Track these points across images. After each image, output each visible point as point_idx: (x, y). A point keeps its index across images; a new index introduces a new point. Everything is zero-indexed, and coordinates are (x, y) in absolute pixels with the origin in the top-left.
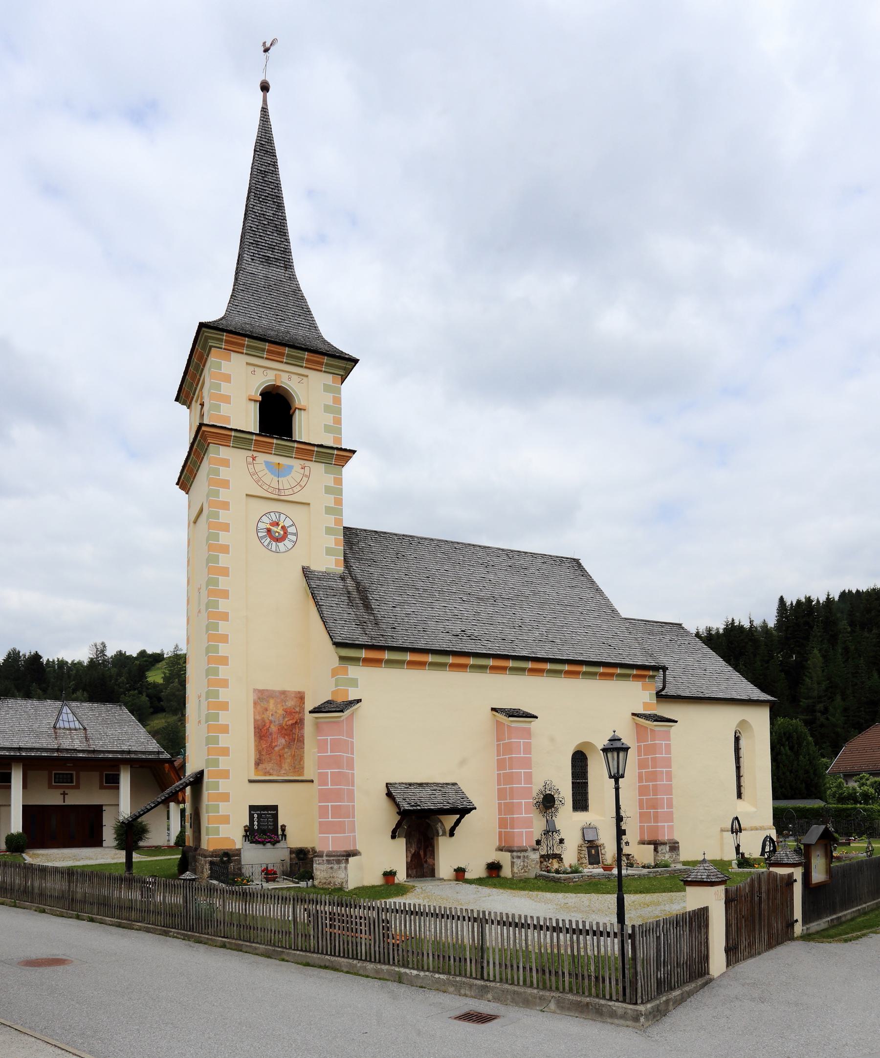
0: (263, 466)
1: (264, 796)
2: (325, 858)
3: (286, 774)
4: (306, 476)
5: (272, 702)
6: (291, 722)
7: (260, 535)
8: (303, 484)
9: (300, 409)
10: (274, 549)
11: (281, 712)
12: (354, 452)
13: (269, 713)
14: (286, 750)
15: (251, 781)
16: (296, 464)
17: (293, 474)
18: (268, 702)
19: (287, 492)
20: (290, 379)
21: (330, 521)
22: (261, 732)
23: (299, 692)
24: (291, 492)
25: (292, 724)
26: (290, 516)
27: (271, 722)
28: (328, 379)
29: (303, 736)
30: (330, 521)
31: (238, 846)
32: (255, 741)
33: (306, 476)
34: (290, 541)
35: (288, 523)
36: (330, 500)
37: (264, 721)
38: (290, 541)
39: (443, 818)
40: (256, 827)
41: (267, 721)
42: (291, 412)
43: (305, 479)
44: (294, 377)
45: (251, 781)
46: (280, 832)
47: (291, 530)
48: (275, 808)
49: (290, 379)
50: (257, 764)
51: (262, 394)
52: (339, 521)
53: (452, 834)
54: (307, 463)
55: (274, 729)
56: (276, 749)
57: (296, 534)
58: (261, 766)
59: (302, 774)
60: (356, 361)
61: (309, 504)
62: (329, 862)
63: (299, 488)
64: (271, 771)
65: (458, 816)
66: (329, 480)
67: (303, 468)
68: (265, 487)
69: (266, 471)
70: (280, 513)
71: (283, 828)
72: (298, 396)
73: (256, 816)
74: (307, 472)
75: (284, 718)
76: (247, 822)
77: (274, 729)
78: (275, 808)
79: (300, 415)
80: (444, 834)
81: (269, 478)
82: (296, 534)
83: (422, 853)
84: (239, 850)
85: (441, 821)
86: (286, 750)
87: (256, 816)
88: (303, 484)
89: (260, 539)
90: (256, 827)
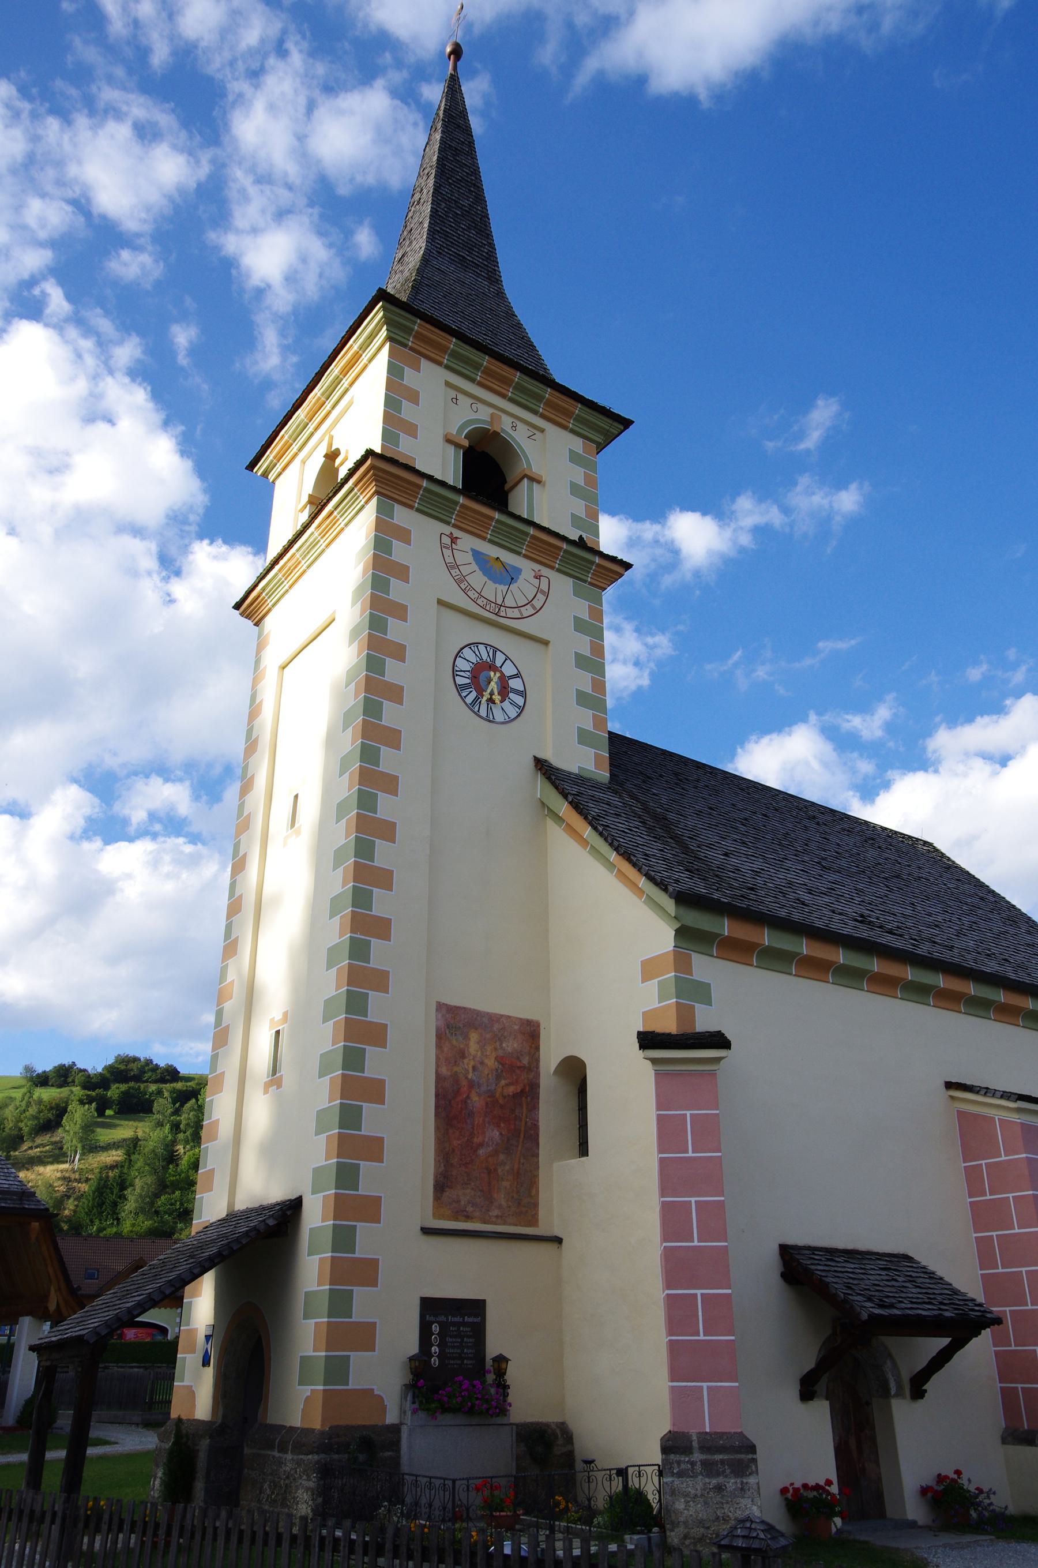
0: (469, 558)
1: (458, 1271)
2: (697, 1456)
3: (502, 1219)
4: (543, 592)
5: (474, 1037)
6: (511, 1090)
7: (460, 681)
8: (537, 604)
9: (532, 479)
10: (483, 712)
11: (491, 1062)
13: (468, 1063)
14: (502, 1157)
15: (426, 1231)
16: (527, 568)
17: (521, 582)
18: (466, 1037)
19: (510, 613)
22: (451, 1106)
23: (529, 1022)
24: (516, 613)
25: (515, 1096)
27: (471, 1084)
28: (577, 444)
29: (535, 1127)
31: (391, 1417)
32: (437, 1128)
33: (543, 592)
34: (513, 704)
35: (508, 670)
36: (583, 644)
37: (455, 1077)
38: (513, 704)
39: (892, 1343)
40: (435, 1361)
41: (464, 1083)
42: (507, 487)
43: (541, 597)
44: (520, 426)
45: (426, 1231)
46: (490, 1378)
48: (477, 1307)
50: (441, 1186)
53: (918, 1393)
54: (545, 571)
55: (476, 1101)
56: (481, 1152)
57: (523, 694)
58: (448, 1194)
59: (533, 1222)
60: (627, 423)
61: (546, 643)
62: (710, 1469)
63: (528, 611)
64: (470, 1209)
65: (946, 1341)
66: (582, 608)
67: (538, 577)
68: (473, 594)
69: (474, 567)
70: (496, 650)
71: (501, 1360)
72: (526, 456)
73: (435, 1328)
74: (544, 587)
75: (498, 1078)
76: (414, 1349)
77: (476, 1101)
78: (477, 1307)
79: (530, 490)
80: (899, 1394)
81: (477, 579)
82: (523, 694)
83: (853, 1444)
84: (396, 1429)
85: (890, 1356)
86: (502, 1157)
87: (435, 1328)
89: (460, 688)
90: (435, 1361)
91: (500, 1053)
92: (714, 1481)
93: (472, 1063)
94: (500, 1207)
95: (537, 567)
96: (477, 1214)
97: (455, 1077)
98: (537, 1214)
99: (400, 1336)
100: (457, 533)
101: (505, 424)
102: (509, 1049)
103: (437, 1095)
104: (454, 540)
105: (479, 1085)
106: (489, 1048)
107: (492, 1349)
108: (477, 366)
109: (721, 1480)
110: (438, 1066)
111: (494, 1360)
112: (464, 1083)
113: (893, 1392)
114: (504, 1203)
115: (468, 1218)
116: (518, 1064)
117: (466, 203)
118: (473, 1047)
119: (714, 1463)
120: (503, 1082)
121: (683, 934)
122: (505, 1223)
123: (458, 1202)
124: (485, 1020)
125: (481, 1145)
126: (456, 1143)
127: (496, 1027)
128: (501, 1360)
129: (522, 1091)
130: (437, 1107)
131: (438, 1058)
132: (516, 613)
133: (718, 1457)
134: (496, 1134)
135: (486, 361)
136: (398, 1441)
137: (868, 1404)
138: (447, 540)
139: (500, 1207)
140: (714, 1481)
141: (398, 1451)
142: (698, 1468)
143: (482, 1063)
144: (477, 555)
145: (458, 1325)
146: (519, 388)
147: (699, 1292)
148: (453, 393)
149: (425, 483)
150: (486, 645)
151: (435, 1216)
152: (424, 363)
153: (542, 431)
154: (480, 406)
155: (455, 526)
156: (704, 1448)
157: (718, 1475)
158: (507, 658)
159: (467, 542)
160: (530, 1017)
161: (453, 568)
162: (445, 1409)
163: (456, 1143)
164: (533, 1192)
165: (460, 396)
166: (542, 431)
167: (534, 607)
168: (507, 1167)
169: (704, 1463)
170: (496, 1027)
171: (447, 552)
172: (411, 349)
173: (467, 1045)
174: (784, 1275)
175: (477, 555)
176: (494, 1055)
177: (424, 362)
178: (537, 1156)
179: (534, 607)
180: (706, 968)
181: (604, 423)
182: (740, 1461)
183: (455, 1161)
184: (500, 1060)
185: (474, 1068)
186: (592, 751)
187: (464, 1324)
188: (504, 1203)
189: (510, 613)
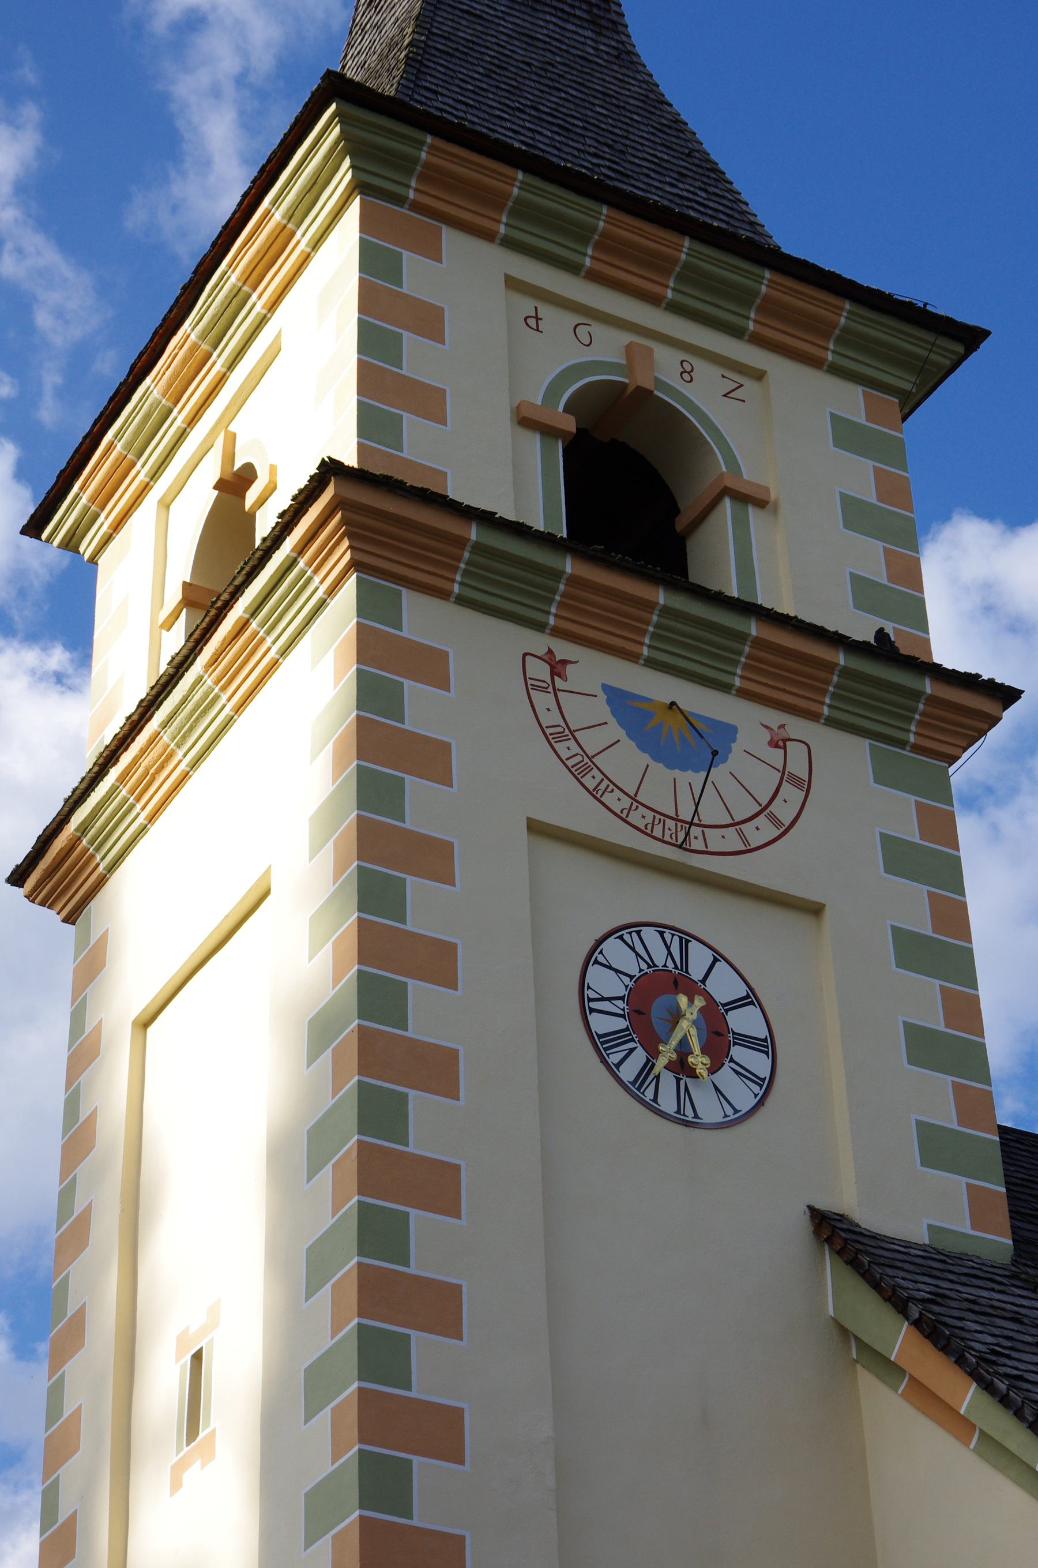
7: (601, 1024)
8: (784, 812)
10: (668, 1102)
16: (749, 721)
17: (736, 760)
19: (716, 840)
20: (687, 374)
26: (738, 951)
28: (851, 401)
34: (744, 1073)
35: (724, 987)
36: (912, 906)
38: (744, 1073)
42: (681, 523)
44: (700, 366)
47: (744, 1021)
49: (687, 374)
54: (796, 727)
57: (766, 1046)
60: (971, 338)
61: (815, 910)
63: (761, 831)
66: (900, 814)
67: (779, 743)
69: (614, 731)
70: (686, 938)
74: (798, 767)
79: (741, 526)
81: (625, 761)
82: (766, 1046)
88: (784, 812)
89: (602, 1044)
95: (775, 718)
100: (563, 650)
101: (666, 367)
104: (557, 667)
108: (581, 234)
135: (603, 218)
138: (540, 671)
144: (619, 701)
146: (690, 276)
148: (527, 305)
149: (473, 533)
150: (661, 928)
153: (759, 376)
154: (599, 330)
155: (557, 632)
159: (592, 670)
161: (561, 737)
165: (546, 312)
166: (759, 376)
175: (619, 701)
177: (449, 236)
181: (913, 342)
186: (957, 1184)
189: (716, 840)
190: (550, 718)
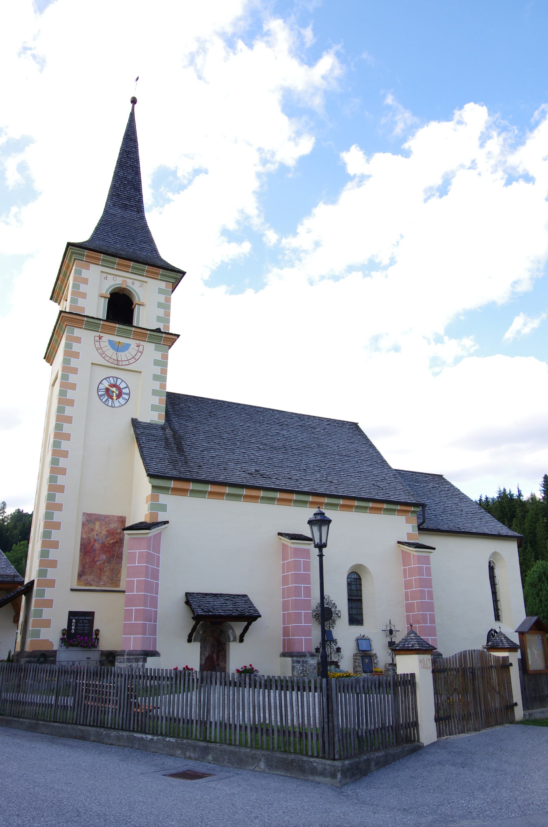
0: (107, 344)
1: (83, 603)
2: (126, 657)
3: (104, 585)
4: (140, 352)
5: (98, 523)
6: (112, 541)
7: (100, 393)
8: (137, 357)
9: (138, 304)
10: (110, 404)
11: (104, 532)
12: (178, 336)
13: (94, 533)
14: (106, 564)
15: (72, 590)
16: (133, 343)
17: (130, 350)
18: (94, 524)
19: (124, 363)
20: (133, 284)
21: (156, 385)
22: (86, 549)
23: (121, 517)
24: (127, 363)
25: (113, 543)
26: (126, 379)
27: (95, 540)
28: (163, 285)
29: (121, 554)
30: (156, 385)
31: (56, 648)
32: (80, 556)
33: (140, 352)
34: (124, 399)
36: (157, 370)
37: (89, 539)
39: (233, 624)
40: (73, 631)
41: (92, 540)
43: (139, 354)
44: (136, 282)
45: (72, 590)
46: (94, 636)
47: (126, 391)
48: (92, 614)
49: (133, 284)
50: (80, 575)
51: (112, 294)
52: (164, 386)
53: (241, 640)
54: (142, 343)
55: (97, 546)
56: (98, 563)
57: (129, 394)
58: (83, 578)
59: (118, 586)
61: (141, 372)
62: (129, 660)
63: (133, 360)
64: (92, 582)
65: (246, 623)
66: (158, 356)
67: (138, 346)
68: (107, 358)
69: (109, 347)
70: (117, 378)
71: (98, 631)
73: (74, 621)
75: (107, 537)
76: (65, 626)
77: (97, 546)
78: (92, 614)
79: (139, 309)
80: (234, 640)
81: (110, 352)
83: (215, 656)
84: (56, 651)
85: (232, 629)
86: (106, 564)
87: (74, 621)
88: (137, 357)
89: (100, 396)
90: (73, 631)
91: (108, 529)
92: (129, 664)
93: (96, 533)
94: (104, 581)
95: (138, 342)
96: (95, 584)
97: (89, 539)
98: (120, 583)
99: (61, 623)
100: (102, 335)
101: (129, 282)
102: (112, 527)
103: (81, 545)
104: (100, 338)
105: (98, 540)
106: (103, 527)
107: (95, 628)
108: (114, 263)
109: (131, 664)
110: (82, 534)
111: (96, 631)
112: (92, 540)
113: (231, 640)
114: (106, 580)
115: (91, 585)
116: (116, 532)
117: (130, 177)
118: (97, 527)
119: (130, 659)
120: (109, 539)
121: (154, 487)
122: (106, 587)
123: (87, 580)
124: (103, 517)
125: (98, 561)
126: (87, 560)
127: (107, 519)
128: (98, 631)
129: (117, 542)
130: (81, 549)
131: (82, 532)
132: (127, 363)
133: (132, 657)
134: (104, 557)
135: (117, 260)
136: (56, 655)
137: (225, 644)
138: (97, 338)
139: (104, 581)
140: (129, 664)
141: (56, 658)
142: (125, 660)
143: (100, 533)
144: (110, 342)
145: (83, 620)
146: (133, 268)
147: (134, 608)
148: (105, 275)
149: (85, 319)
150: (113, 377)
151: (77, 585)
152: (92, 266)
153: (146, 282)
154: (118, 278)
155: (101, 332)
156: (128, 655)
157: (131, 662)
158: (123, 381)
159: (106, 337)
160: (122, 515)
161: (99, 349)
162: (73, 646)
163: (87, 560)
164: (119, 576)
165: (109, 276)
166: (146, 282)
167: (135, 359)
168: (108, 568)
169: (127, 659)
170: (107, 519)
171: (97, 343)
172: (85, 261)
173: (95, 527)
174: (186, 602)
175: (110, 342)
176: (106, 529)
177: (91, 265)
178: (121, 563)
179: (135, 359)
180: (164, 498)
181: (173, 274)
182: (138, 658)
183: (87, 566)
184: (108, 531)
185: (97, 535)
186: (157, 413)
187: (85, 619)
188: (106, 580)
189: (124, 363)
190: (98, 346)
